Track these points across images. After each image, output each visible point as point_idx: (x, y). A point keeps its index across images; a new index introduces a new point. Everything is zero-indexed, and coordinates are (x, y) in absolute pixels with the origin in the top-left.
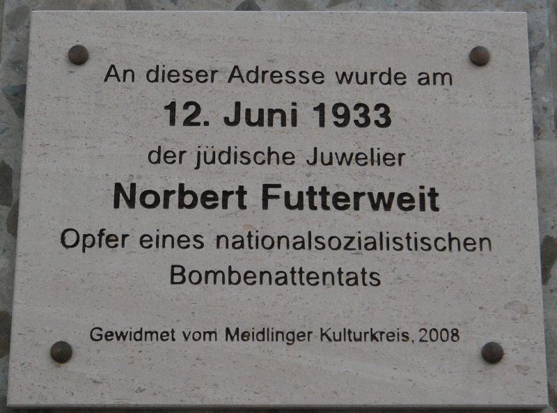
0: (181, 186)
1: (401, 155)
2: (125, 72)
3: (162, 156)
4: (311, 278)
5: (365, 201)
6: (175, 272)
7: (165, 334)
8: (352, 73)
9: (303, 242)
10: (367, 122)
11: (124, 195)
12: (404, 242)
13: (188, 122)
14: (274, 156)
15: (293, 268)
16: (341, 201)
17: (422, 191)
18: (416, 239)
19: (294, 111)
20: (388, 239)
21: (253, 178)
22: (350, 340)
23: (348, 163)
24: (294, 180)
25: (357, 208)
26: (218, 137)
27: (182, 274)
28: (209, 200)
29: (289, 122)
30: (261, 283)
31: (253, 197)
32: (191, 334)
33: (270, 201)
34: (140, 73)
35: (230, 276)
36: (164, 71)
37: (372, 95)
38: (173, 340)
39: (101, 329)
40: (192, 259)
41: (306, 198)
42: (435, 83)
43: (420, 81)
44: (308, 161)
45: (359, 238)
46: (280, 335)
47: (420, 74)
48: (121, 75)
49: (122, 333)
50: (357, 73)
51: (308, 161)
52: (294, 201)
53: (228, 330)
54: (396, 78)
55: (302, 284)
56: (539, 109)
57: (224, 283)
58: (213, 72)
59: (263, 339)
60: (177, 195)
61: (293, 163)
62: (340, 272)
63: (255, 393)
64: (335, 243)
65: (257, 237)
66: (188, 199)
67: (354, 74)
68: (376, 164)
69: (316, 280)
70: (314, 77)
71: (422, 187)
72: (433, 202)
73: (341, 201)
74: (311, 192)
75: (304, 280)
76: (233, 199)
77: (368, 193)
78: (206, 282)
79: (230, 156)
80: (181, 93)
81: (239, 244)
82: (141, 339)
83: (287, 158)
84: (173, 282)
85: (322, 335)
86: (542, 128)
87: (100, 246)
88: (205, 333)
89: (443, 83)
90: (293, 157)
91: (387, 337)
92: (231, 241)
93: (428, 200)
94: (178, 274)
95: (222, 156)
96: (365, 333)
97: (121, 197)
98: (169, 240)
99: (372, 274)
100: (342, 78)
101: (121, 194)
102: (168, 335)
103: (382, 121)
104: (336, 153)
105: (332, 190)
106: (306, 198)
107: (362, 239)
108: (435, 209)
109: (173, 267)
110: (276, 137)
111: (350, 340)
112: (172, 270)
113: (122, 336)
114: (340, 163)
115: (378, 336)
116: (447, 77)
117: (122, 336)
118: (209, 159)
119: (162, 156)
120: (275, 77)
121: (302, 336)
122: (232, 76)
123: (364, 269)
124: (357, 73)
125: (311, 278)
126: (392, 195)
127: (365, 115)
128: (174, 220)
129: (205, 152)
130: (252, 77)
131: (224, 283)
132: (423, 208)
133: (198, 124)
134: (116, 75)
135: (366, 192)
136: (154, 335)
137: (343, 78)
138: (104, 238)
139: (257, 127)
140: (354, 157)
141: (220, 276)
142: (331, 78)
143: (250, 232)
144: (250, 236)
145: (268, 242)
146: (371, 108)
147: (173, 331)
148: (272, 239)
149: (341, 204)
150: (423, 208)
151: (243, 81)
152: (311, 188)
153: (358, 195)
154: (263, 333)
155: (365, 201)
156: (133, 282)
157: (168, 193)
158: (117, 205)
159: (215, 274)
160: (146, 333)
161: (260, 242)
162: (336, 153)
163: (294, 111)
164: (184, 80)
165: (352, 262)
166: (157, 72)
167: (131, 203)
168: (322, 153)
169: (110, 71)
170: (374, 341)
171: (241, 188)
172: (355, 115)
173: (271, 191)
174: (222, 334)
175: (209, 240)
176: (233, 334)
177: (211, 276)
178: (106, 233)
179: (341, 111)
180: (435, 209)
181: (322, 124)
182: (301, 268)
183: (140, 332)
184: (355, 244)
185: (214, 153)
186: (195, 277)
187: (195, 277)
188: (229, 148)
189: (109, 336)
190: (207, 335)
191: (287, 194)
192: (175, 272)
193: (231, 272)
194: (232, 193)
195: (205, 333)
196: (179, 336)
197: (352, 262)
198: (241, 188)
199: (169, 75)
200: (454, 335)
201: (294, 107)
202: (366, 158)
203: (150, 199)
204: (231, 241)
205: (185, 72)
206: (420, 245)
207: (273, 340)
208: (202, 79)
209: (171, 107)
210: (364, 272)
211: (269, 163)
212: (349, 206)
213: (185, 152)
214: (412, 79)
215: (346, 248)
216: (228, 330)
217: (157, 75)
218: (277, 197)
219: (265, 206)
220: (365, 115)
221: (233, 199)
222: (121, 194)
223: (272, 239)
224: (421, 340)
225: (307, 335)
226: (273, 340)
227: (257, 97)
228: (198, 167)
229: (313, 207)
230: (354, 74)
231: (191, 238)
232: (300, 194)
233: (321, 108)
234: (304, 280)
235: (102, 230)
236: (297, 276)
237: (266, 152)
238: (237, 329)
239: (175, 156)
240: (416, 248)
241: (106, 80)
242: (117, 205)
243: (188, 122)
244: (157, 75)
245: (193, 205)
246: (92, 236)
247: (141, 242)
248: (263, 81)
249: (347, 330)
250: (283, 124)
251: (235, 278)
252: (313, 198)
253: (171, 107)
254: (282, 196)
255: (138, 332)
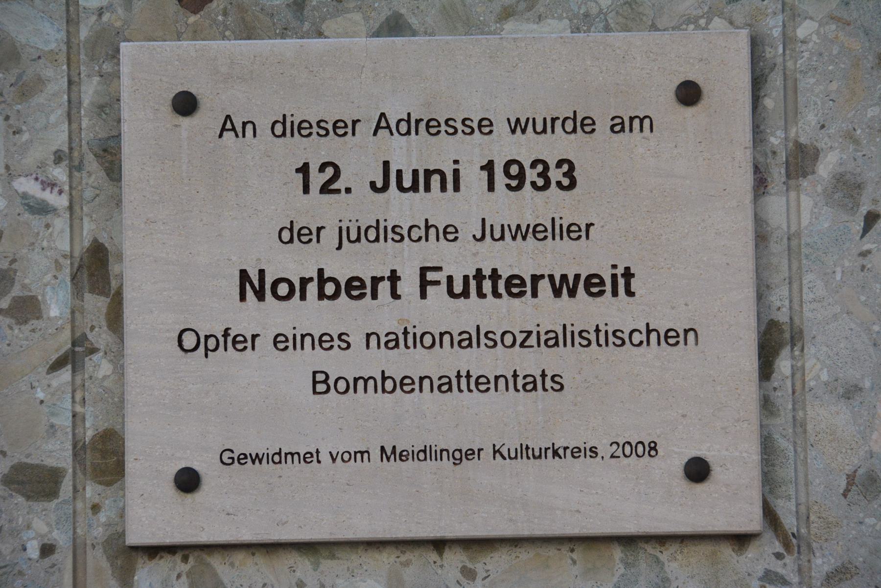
0: (321, 272)
1: (589, 226)
2: (244, 124)
3: (296, 234)
4: (481, 384)
5: (544, 286)
6: (317, 379)
7: (308, 455)
8: (528, 119)
9: (470, 339)
10: (547, 186)
11: (252, 285)
12: (592, 337)
13: (325, 189)
14: (432, 231)
15: (459, 372)
16: (515, 286)
17: (614, 271)
18: (606, 332)
19: (456, 172)
20: (573, 332)
21: (408, 260)
22: (528, 458)
23: (524, 238)
24: (458, 260)
25: (535, 294)
26: (360, 207)
27: (325, 381)
28: (354, 287)
29: (450, 185)
30: (421, 390)
31: (409, 285)
32: (340, 455)
33: (429, 288)
34: (263, 127)
35: (384, 383)
36: (292, 122)
37: (555, 146)
38: (319, 462)
39: (232, 451)
40: (336, 363)
41: (473, 284)
42: (631, 130)
43: (612, 127)
44: (474, 236)
45: (538, 332)
46: (445, 453)
47: (613, 119)
48: (239, 129)
49: (257, 455)
50: (534, 119)
51: (474, 236)
52: (458, 288)
53: (383, 449)
54: (583, 125)
55: (470, 390)
56: (766, 155)
57: (376, 391)
58: (355, 122)
59: (425, 459)
60: (316, 280)
61: (456, 238)
62: (515, 376)
63: (417, 523)
64: (508, 339)
65: (415, 334)
66: (330, 289)
67: (531, 121)
68: (558, 237)
69: (487, 386)
70: (480, 126)
71: (614, 267)
72: (628, 285)
73: (515, 286)
74: (479, 276)
75: (473, 386)
76: (384, 288)
77: (549, 276)
78: (355, 391)
79: (380, 232)
80: (317, 149)
81: (393, 342)
82: (280, 462)
83: (449, 233)
84: (315, 392)
85: (495, 452)
86: (769, 179)
87: (226, 350)
88: (356, 453)
89: (641, 130)
90: (457, 231)
91: (572, 452)
92: (383, 340)
93: (621, 282)
94: (321, 383)
95: (369, 232)
96: (546, 449)
98: (308, 340)
99: (553, 377)
100: (516, 126)
101: (247, 284)
102: (312, 456)
103: (566, 182)
104: (509, 226)
105: (505, 273)
106: (473, 284)
107: (542, 333)
108: (630, 293)
109: (315, 373)
110: (432, 206)
111: (528, 458)
112: (314, 377)
113: (257, 459)
114: (514, 238)
115: (561, 452)
116: (647, 122)
117: (257, 459)
118: (353, 237)
119: (296, 234)
120: (432, 126)
121: (470, 454)
122: (378, 127)
123: (543, 371)
124: (534, 119)
125: (481, 384)
126: (577, 277)
127: (544, 175)
128: (311, 315)
129: (348, 228)
130: (403, 128)
131: (376, 391)
132: (615, 293)
133: (338, 191)
134: (233, 129)
135: (546, 275)
136: (296, 456)
137: (517, 126)
138: (230, 339)
139: (411, 193)
140: (531, 230)
141: (371, 383)
142: (501, 128)
143: (406, 328)
144: (406, 333)
145: (428, 340)
146: (552, 164)
147: (318, 452)
148: (433, 336)
149: (515, 290)
150: (615, 293)
151: (392, 134)
152: (479, 271)
153: (536, 279)
154: (424, 451)
155: (544, 286)
156: (268, 392)
157: (304, 282)
158: (243, 298)
159: (366, 381)
160: (286, 454)
161: (418, 340)
162: (509, 226)
163: (456, 172)
164: (318, 133)
165: (530, 362)
166: (284, 124)
167: (260, 295)
168: (492, 226)
169: (225, 123)
170: (557, 458)
171: (393, 272)
172: (531, 175)
173: (430, 276)
174: (376, 453)
175: (357, 339)
176: (389, 454)
177: (361, 383)
178: (232, 333)
179: (514, 170)
180: (630, 293)
181: (491, 187)
182: (468, 372)
183: (279, 454)
184: (533, 340)
185: (359, 228)
186: (342, 385)
187: (342, 385)
188: (378, 221)
189: (242, 459)
190: (359, 455)
191: (450, 279)
192: (317, 379)
193: (384, 379)
194: (382, 279)
195: (356, 453)
196: (325, 457)
197: (530, 362)
198: (393, 272)
199: (300, 128)
200: (651, 449)
201: (456, 167)
202: (546, 230)
203: (283, 289)
204: (383, 340)
205: (318, 123)
206: (611, 339)
207: (436, 459)
208: (341, 132)
209: (304, 170)
210: (543, 375)
211: (427, 240)
212: (525, 292)
213: (323, 227)
214: (603, 126)
215: (522, 345)
216: (383, 449)
217: (287, 127)
218: (437, 283)
219: (423, 295)
220: (544, 175)
221: (384, 288)
222: (247, 284)
223: (433, 336)
224: (612, 456)
225: (476, 452)
226: (436, 459)
227: (407, 154)
228: (339, 248)
229: (481, 295)
230: (531, 121)
231: (335, 337)
232: (466, 278)
233: (489, 167)
234: (473, 386)
235: (227, 330)
236: (464, 381)
237: (422, 225)
238: (394, 447)
239: (311, 233)
240: (607, 345)
241: (221, 136)
242: (243, 298)
243: (325, 189)
244: (287, 127)
245: (336, 295)
246: (215, 336)
247: (275, 343)
248: (417, 133)
249: (524, 447)
250: (443, 188)
251: (389, 385)
252: (479, 284)
253: (304, 170)
254: (444, 281)
255: (276, 454)
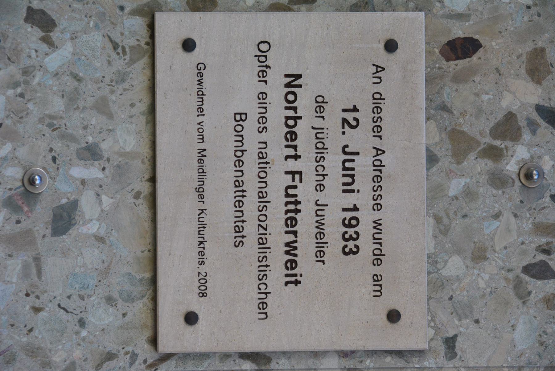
0: (300, 118)
1: (323, 262)
2: (380, 78)
3: (320, 105)
4: (239, 203)
5: (291, 238)
8: (381, 230)
9: (263, 197)
10: (345, 240)
11: (293, 81)
12: (263, 263)
13: (345, 121)
14: (321, 178)
15: (245, 191)
16: (291, 222)
17: (298, 275)
18: (266, 271)
19: (353, 191)
20: (266, 252)
21: (305, 164)
22: (199, 228)
23: (317, 227)
24: (305, 191)
25: (287, 232)
26: (335, 139)
27: (241, 119)
28: (291, 136)
29: (346, 188)
30: (236, 171)
31: (292, 165)
33: (291, 175)
34: (379, 88)
36: (381, 103)
37: (366, 244)
38: (198, 116)
39: (204, 69)
40: (250, 127)
41: (293, 199)
42: (374, 285)
43: (376, 275)
44: (318, 200)
45: (266, 234)
46: (202, 183)
47: (380, 275)
48: (377, 75)
49: (202, 83)
50: (381, 233)
51: (318, 200)
52: (290, 191)
54: (378, 260)
55: (235, 197)
56: (361, 358)
57: (236, 147)
58: (380, 137)
59: (199, 173)
60: (296, 115)
61: (317, 191)
62: (243, 221)
65: (266, 168)
66: (291, 122)
67: (380, 231)
68: (317, 245)
69: (238, 206)
70: (377, 204)
71: (301, 275)
72: (291, 282)
73: (291, 222)
74: (297, 203)
75: (237, 198)
76: (292, 152)
78: (236, 136)
79: (321, 150)
80: (365, 116)
81: (262, 156)
82: (198, 95)
83: (320, 187)
84: (235, 114)
85: (202, 210)
86: (347, 359)
87: (259, 66)
88: (203, 135)
89: (374, 291)
90: (321, 191)
91: (202, 251)
93: (293, 279)
95: (321, 144)
96: (203, 238)
97: (292, 79)
98: (264, 110)
99: (242, 242)
100: (377, 223)
102: (201, 112)
103: (347, 250)
104: (324, 219)
105: (298, 216)
106: (293, 199)
107: (266, 236)
108: (287, 283)
109: (246, 114)
110: (335, 179)
111: (199, 228)
112: (243, 114)
113: (200, 83)
114: (317, 222)
115: (202, 245)
116: (379, 294)
117: (200, 83)
118: (319, 135)
119: (320, 105)
120: (378, 178)
121: (201, 197)
122: (378, 149)
123: (245, 237)
124: (381, 233)
125: (239, 203)
126: (296, 255)
128: (277, 112)
129: (324, 133)
130: (377, 163)
131: (236, 147)
132: (287, 275)
133: (343, 128)
134: (377, 72)
136: (201, 103)
137: (377, 224)
138: (264, 69)
139: (342, 167)
140: (321, 231)
141: (240, 144)
142: (376, 216)
143: (269, 163)
144: (267, 163)
145: (263, 175)
146: (356, 243)
147: (203, 115)
149: (289, 222)
150: (287, 275)
151: (374, 157)
153: (295, 233)
154: (203, 172)
155: (291, 238)
158: (287, 76)
159: (241, 141)
160: (202, 98)
161: (263, 170)
162: (324, 219)
163: (353, 191)
164: (374, 117)
165: (251, 229)
166: (380, 99)
167: (288, 85)
170: (199, 243)
171: (300, 157)
172: (351, 231)
173: (297, 177)
174: (202, 146)
175: (264, 137)
176: (202, 153)
177: (240, 139)
178: (268, 70)
179: (354, 222)
180: (287, 283)
181: (344, 210)
182: (245, 196)
184: (262, 231)
185: (323, 139)
187: (239, 128)
188: (327, 149)
190: (201, 137)
191: (295, 187)
193: (242, 151)
194: (296, 151)
195: (203, 135)
196: (201, 119)
197: (251, 229)
198: (300, 157)
199: (377, 107)
200: (203, 294)
201: (356, 191)
202: (321, 239)
203: (291, 97)
204: (263, 151)
205: (380, 118)
206: (262, 273)
208: (375, 129)
210: (243, 237)
211: (317, 175)
212: (288, 227)
213: (324, 119)
214: (377, 270)
215: (259, 225)
217: (378, 100)
218: (293, 180)
219: (287, 173)
221: (292, 152)
224: (199, 273)
227: (363, 165)
228: (313, 128)
229: (287, 204)
230: (380, 231)
231: (265, 125)
232: (296, 196)
234: (237, 198)
235: (270, 67)
236: (241, 194)
237: (324, 173)
238: (205, 156)
239: (321, 113)
240: (260, 271)
241: (374, 65)
242: (287, 76)
243: (345, 121)
244: (378, 100)
245: (287, 125)
247: (262, 93)
248: (374, 170)
249: (205, 226)
250: (344, 184)
252: (293, 203)
254: (294, 184)
